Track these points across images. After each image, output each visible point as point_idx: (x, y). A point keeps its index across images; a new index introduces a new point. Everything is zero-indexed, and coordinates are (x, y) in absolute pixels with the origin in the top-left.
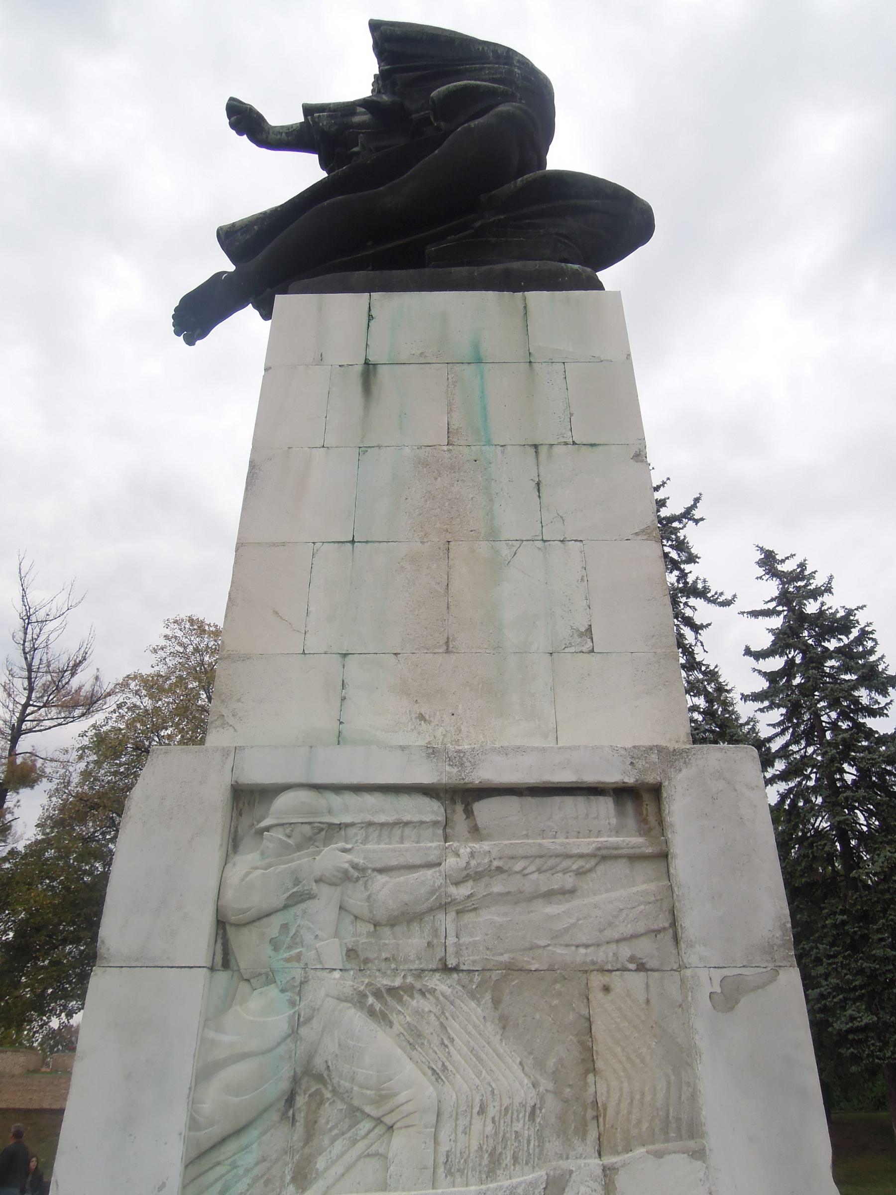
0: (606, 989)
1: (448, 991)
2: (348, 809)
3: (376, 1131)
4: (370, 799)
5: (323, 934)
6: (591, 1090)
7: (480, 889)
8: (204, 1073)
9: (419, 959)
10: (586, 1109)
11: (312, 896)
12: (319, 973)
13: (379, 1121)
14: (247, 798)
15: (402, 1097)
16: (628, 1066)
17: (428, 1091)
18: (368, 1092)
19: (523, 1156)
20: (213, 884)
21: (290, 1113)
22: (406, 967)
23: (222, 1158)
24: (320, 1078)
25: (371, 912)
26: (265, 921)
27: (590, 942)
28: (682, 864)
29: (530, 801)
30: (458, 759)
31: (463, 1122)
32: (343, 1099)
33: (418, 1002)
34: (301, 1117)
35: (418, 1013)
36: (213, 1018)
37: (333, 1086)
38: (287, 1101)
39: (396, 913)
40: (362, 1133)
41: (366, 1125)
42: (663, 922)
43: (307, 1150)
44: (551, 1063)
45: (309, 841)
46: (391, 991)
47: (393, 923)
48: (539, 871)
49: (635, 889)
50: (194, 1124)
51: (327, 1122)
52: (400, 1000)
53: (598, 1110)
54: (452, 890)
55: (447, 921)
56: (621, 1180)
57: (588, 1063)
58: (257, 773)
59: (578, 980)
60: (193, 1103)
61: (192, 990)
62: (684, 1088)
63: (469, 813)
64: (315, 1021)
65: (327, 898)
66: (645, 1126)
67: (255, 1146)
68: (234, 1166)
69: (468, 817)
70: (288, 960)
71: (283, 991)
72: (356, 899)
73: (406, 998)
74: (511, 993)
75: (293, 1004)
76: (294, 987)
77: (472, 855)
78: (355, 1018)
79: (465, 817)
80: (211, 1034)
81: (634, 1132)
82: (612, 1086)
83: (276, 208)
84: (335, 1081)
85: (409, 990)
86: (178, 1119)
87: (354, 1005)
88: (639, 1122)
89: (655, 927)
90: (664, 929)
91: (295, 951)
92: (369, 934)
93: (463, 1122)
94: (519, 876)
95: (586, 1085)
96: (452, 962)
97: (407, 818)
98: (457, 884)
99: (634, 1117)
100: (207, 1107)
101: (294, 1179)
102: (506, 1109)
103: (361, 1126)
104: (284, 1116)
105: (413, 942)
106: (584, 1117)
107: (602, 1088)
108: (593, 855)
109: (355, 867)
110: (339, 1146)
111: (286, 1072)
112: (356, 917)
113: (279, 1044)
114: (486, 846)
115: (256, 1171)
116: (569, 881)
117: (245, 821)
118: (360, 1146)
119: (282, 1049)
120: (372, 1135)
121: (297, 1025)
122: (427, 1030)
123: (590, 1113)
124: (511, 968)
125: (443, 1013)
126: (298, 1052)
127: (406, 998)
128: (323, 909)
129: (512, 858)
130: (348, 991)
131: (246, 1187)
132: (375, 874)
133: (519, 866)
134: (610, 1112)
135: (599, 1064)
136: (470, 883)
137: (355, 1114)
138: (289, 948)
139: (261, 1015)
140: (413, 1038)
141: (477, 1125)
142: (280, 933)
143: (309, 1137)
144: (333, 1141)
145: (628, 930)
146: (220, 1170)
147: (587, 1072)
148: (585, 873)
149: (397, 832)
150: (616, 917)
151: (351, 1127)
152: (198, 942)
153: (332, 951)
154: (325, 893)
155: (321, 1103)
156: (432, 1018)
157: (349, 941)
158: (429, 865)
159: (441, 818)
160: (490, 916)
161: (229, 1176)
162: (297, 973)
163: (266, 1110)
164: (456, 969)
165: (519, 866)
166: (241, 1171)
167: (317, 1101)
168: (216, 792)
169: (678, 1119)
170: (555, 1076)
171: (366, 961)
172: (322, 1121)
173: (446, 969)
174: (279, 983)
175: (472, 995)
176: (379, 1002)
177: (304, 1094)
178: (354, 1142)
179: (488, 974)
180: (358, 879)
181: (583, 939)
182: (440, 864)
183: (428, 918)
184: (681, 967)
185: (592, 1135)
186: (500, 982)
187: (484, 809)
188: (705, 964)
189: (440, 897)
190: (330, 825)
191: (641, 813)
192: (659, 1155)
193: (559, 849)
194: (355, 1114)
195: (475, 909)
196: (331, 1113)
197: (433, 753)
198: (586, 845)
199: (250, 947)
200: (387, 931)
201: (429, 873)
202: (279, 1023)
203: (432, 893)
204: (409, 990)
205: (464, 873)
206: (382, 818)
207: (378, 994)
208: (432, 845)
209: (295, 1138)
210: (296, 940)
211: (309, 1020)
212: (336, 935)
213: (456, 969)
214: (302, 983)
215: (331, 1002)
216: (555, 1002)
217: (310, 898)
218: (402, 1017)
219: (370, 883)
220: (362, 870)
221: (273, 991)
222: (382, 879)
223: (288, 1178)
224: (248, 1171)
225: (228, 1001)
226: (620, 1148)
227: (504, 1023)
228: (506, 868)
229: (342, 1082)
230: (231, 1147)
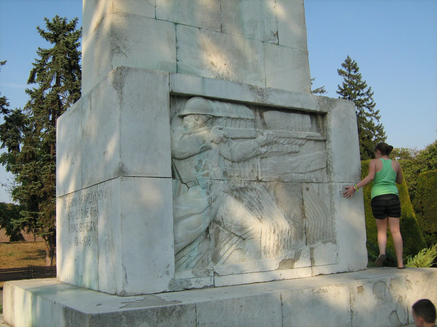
1: (260, 189)
2: (218, 109)
3: (239, 241)
4: (227, 106)
6: (304, 224)
8: (176, 221)
9: (249, 176)
10: (302, 230)
11: (210, 148)
12: (216, 181)
16: (314, 215)
18: (238, 227)
20: (168, 139)
21: (208, 236)
22: (245, 180)
23: (185, 254)
24: (219, 223)
25: (231, 157)
26: (192, 158)
27: (302, 172)
29: (284, 114)
30: (261, 92)
32: (227, 230)
33: (250, 193)
34: (213, 238)
37: (224, 225)
38: (206, 232)
39: (241, 158)
40: (235, 241)
42: (324, 166)
43: (216, 249)
44: (292, 216)
46: (241, 188)
48: (288, 144)
49: (316, 153)
50: (175, 242)
51: (222, 238)
52: (244, 192)
56: (315, 251)
60: (175, 233)
62: (328, 222)
63: (262, 117)
64: (217, 200)
66: (318, 235)
67: (196, 249)
68: (190, 256)
69: (261, 118)
70: (204, 176)
71: (203, 188)
73: (246, 192)
74: (279, 190)
75: (208, 194)
76: (208, 187)
79: (260, 118)
81: (315, 237)
84: (225, 223)
87: (229, 194)
88: (317, 234)
89: (322, 167)
90: (324, 168)
91: (206, 172)
92: (231, 166)
94: (281, 145)
95: (303, 222)
96: (260, 178)
99: (315, 232)
100: (180, 235)
101: (212, 260)
102: (281, 231)
103: (234, 239)
104: (206, 237)
106: (302, 233)
108: (305, 139)
109: (225, 137)
111: (208, 220)
112: (225, 158)
113: (205, 210)
115: (198, 258)
116: (297, 148)
119: (206, 211)
120: (238, 242)
121: (211, 201)
123: (304, 231)
125: (259, 197)
126: (212, 213)
127: (246, 192)
129: (280, 138)
130: (227, 189)
131: (195, 263)
132: (232, 140)
133: (282, 141)
134: (309, 230)
135: (306, 215)
136: (266, 147)
138: (203, 170)
142: (199, 164)
144: (224, 245)
146: (184, 259)
147: (303, 218)
148: (301, 145)
149: (238, 122)
150: (311, 163)
151: (230, 240)
155: (219, 231)
156: (255, 199)
160: (271, 161)
161: (188, 260)
163: (199, 236)
165: (282, 141)
166: (192, 258)
169: (326, 232)
170: (293, 220)
171: (230, 177)
172: (220, 238)
174: (201, 185)
179: (272, 183)
180: (226, 142)
181: (301, 171)
182: (255, 138)
183: (251, 160)
184: (330, 182)
185: (304, 239)
187: (268, 115)
189: (256, 152)
190: (213, 116)
191: (317, 124)
193: (295, 135)
195: (266, 157)
196: (223, 234)
197: (252, 88)
198: (303, 135)
199: (187, 169)
200: (236, 165)
201: (253, 141)
202: (203, 201)
203: (254, 150)
204: (246, 188)
205: (265, 143)
206: (233, 116)
209: (211, 245)
212: (219, 166)
213: (261, 181)
214: (210, 185)
215: (221, 193)
216: (293, 194)
217: (209, 149)
219: (230, 144)
220: (228, 138)
221: (199, 189)
222: (234, 143)
223: (210, 259)
224: (195, 258)
226: (311, 242)
228: (278, 141)
229: (228, 224)
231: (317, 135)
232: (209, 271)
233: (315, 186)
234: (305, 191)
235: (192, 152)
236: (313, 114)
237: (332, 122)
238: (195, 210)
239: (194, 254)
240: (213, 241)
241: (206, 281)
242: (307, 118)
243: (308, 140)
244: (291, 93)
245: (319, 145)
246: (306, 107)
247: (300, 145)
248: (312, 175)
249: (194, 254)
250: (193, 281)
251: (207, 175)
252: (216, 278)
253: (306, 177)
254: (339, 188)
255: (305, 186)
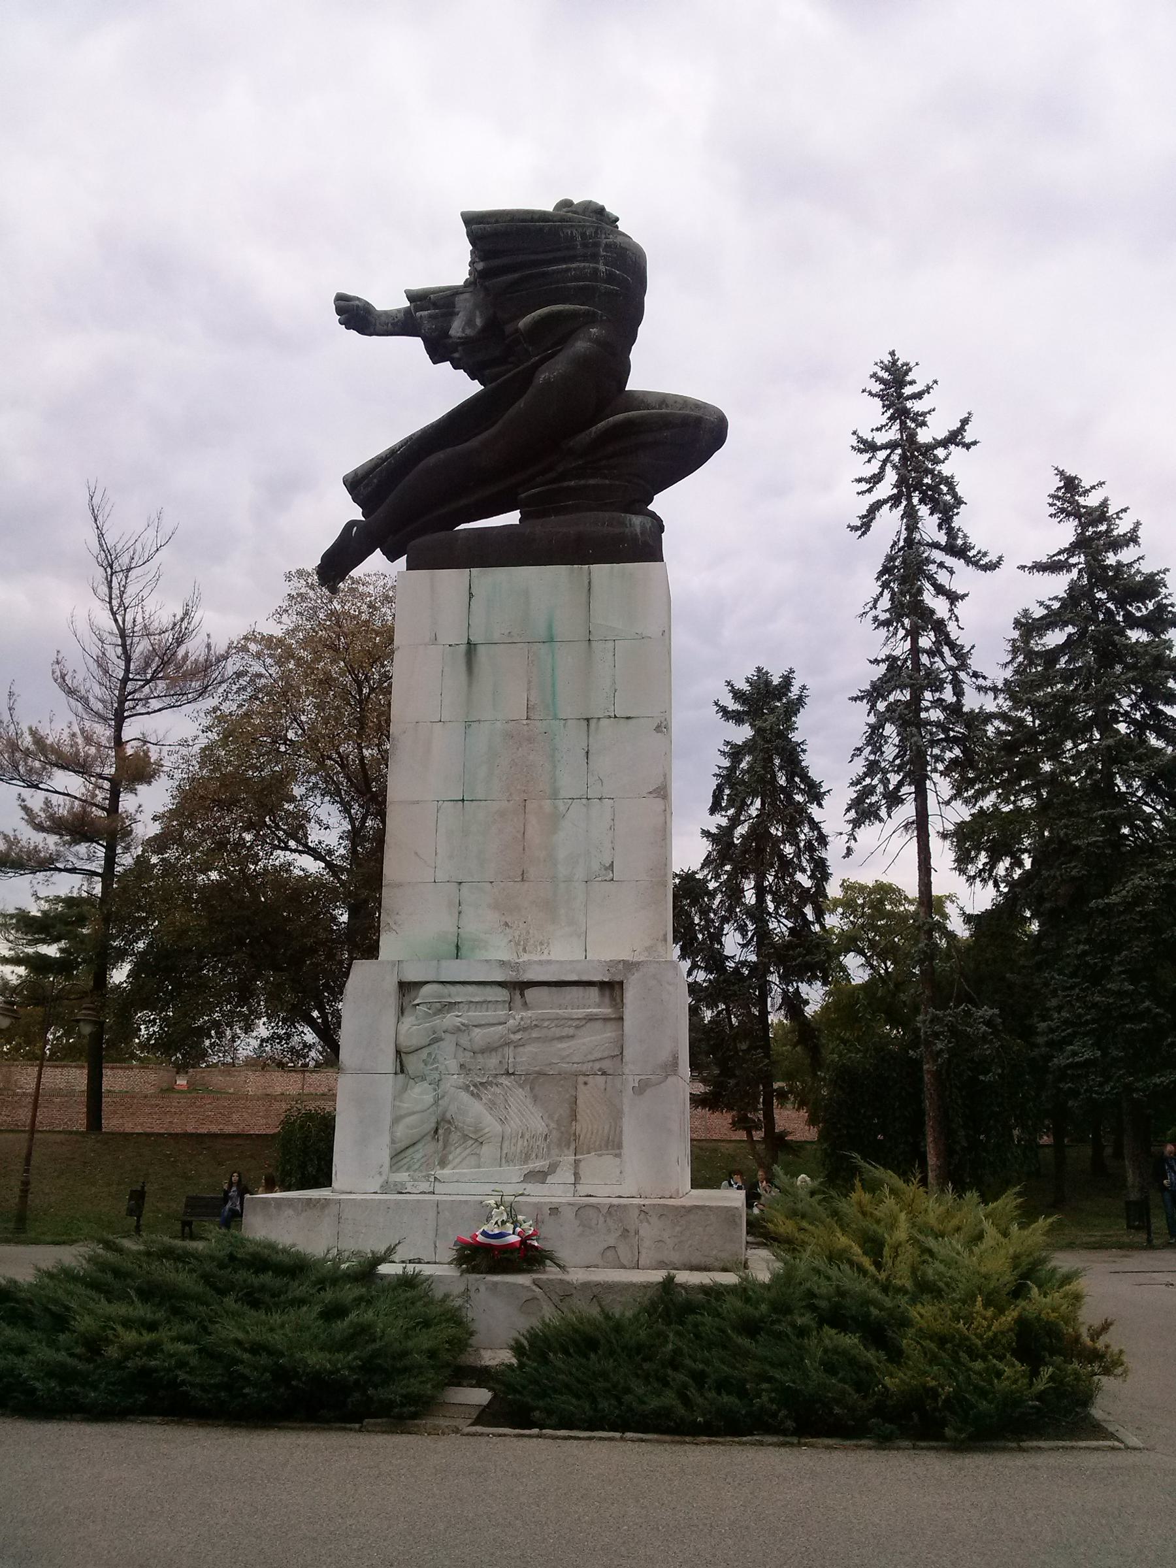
0: (586, 1083)
4: (470, 988)
5: (448, 1058)
7: (526, 1035)
8: (396, 1120)
13: (476, 1140)
14: (406, 988)
15: (486, 1130)
17: (498, 1128)
19: (540, 1155)
28: (627, 1023)
30: (515, 967)
31: (514, 1141)
33: (494, 1089)
34: (441, 1138)
35: (494, 1094)
36: (399, 1095)
41: (470, 1142)
44: (556, 1117)
45: (440, 1011)
46: (481, 1084)
47: (482, 1052)
48: (557, 1026)
50: (393, 1142)
53: (576, 1137)
54: (512, 1036)
55: (509, 1052)
56: (582, 1164)
57: (574, 1116)
58: (411, 976)
59: (573, 1078)
60: (392, 1133)
61: (387, 1084)
63: (522, 995)
65: (450, 1040)
72: (464, 1040)
77: (522, 1019)
78: (464, 1096)
80: (398, 1103)
82: (583, 1126)
83: (392, 452)
85: (491, 1084)
86: (387, 1139)
93: (514, 1141)
97: (489, 999)
98: (514, 1033)
104: (433, 1138)
105: (493, 1061)
107: (578, 1128)
110: (458, 1150)
111: (433, 1120)
114: (529, 1014)
116: (571, 1031)
117: (406, 999)
118: (468, 1151)
122: (498, 1102)
124: (540, 1074)
128: (448, 1045)
133: (546, 1024)
137: (466, 1137)
139: (420, 1095)
140: (492, 1106)
141: (520, 1142)
143: (445, 1147)
145: (599, 1055)
149: (485, 1006)
152: (388, 1061)
153: (453, 1065)
154: (448, 1036)
157: (462, 1061)
158: (501, 1024)
159: (507, 998)
160: (530, 1049)
162: (437, 1077)
164: (513, 1074)
165: (546, 1024)
167: (448, 1132)
168: (390, 985)
173: (508, 1074)
175: (521, 1086)
176: (476, 1089)
177: (442, 1130)
178: (466, 1149)
185: (573, 1147)
186: (534, 1080)
187: (530, 993)
188: (632, 1072)
192: (600, 1155)
194: (466, 1137)
196: (455, 1137)
199: (413, 1064)
202: (429, 1098)
207: (475, 1086)
208: (502, 1013)
210: (435, 1061)
211: (443, 1097)
212: (455, 1057)
213: (513, 1074)
218: (487, 1095)
221: (425, 1084)
222: (477, 1030)
225: (405, 1089)
227: (535, 1099)
230: (410, 1150)
231: (607, 1011)
232: (429, 1176)
233: (600, 1080)
234: (581, 1087)
235: (420, 1045)
236: (603, 986)
237: (630, 994)
238: (418, 1108)
239: (419, 1156)
240: (441, 1142)
241: (424, 1186)
242: (594, 992)
243: (591, 1019)
244: (562, 962)
245: (610, 1026)
246: (585, 978)
247: (577, 1027)
248: (597, 1066)
249: (419, 1156)
250: (409, 1185)
251: (437, 1068)
252: (437, 1183)
253: (585, 1068)
254: (632, 1081)
255: (581, 1079)
